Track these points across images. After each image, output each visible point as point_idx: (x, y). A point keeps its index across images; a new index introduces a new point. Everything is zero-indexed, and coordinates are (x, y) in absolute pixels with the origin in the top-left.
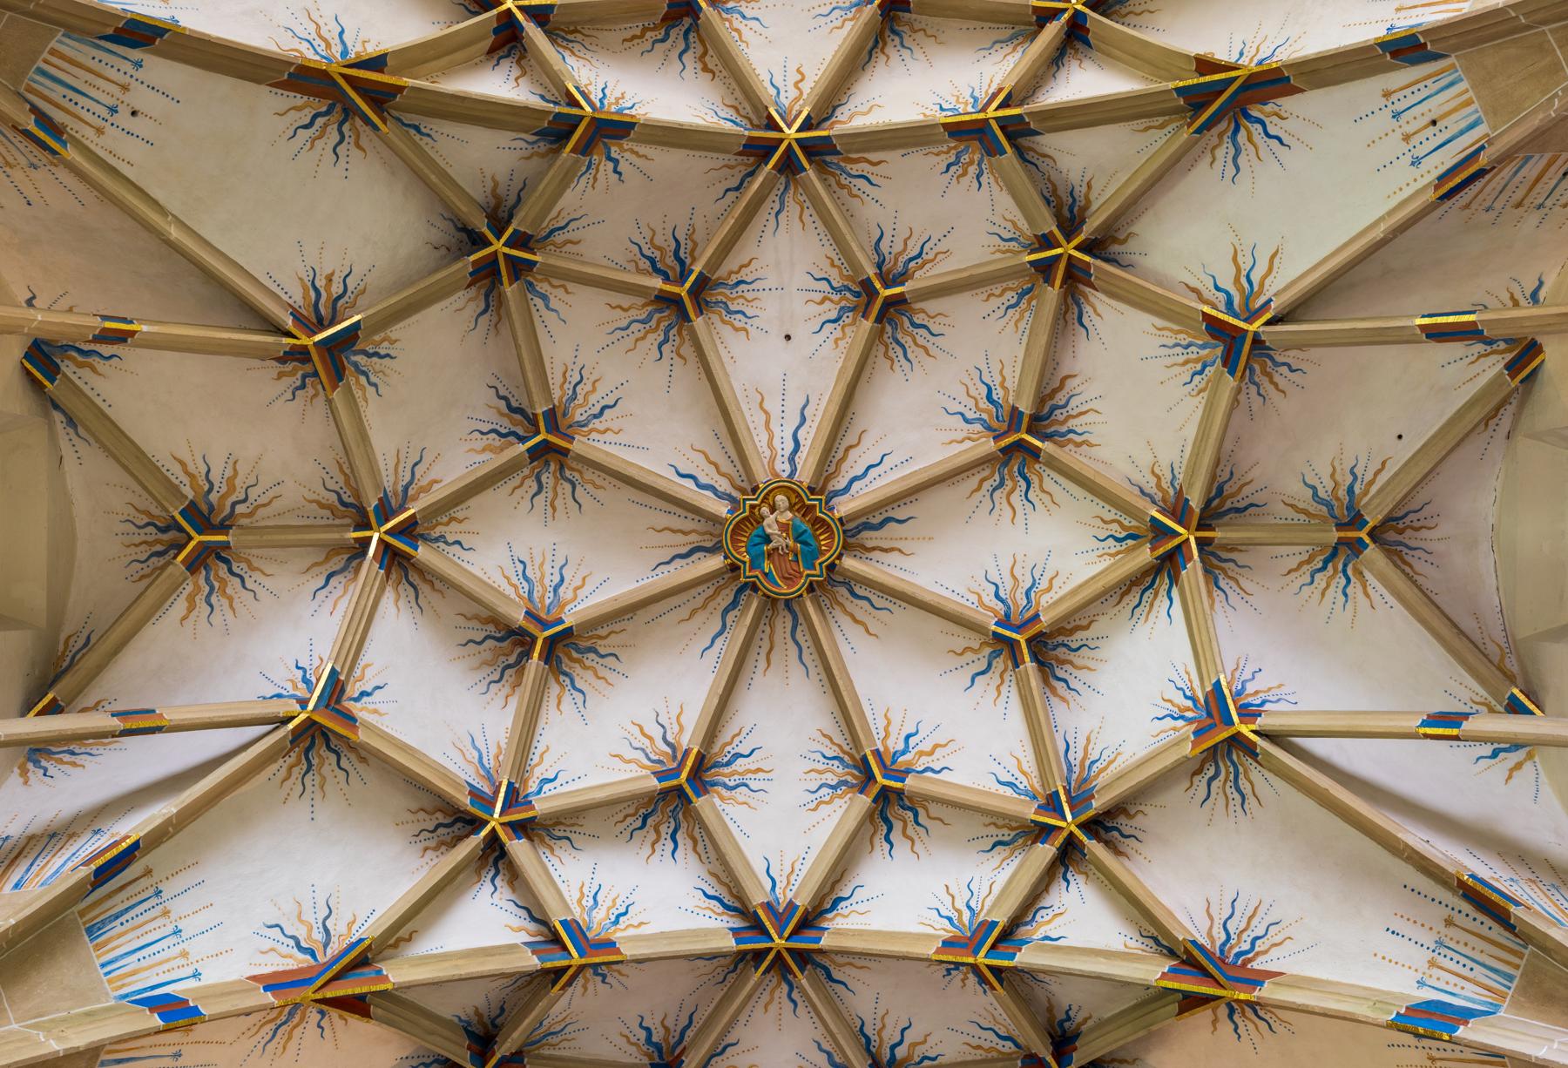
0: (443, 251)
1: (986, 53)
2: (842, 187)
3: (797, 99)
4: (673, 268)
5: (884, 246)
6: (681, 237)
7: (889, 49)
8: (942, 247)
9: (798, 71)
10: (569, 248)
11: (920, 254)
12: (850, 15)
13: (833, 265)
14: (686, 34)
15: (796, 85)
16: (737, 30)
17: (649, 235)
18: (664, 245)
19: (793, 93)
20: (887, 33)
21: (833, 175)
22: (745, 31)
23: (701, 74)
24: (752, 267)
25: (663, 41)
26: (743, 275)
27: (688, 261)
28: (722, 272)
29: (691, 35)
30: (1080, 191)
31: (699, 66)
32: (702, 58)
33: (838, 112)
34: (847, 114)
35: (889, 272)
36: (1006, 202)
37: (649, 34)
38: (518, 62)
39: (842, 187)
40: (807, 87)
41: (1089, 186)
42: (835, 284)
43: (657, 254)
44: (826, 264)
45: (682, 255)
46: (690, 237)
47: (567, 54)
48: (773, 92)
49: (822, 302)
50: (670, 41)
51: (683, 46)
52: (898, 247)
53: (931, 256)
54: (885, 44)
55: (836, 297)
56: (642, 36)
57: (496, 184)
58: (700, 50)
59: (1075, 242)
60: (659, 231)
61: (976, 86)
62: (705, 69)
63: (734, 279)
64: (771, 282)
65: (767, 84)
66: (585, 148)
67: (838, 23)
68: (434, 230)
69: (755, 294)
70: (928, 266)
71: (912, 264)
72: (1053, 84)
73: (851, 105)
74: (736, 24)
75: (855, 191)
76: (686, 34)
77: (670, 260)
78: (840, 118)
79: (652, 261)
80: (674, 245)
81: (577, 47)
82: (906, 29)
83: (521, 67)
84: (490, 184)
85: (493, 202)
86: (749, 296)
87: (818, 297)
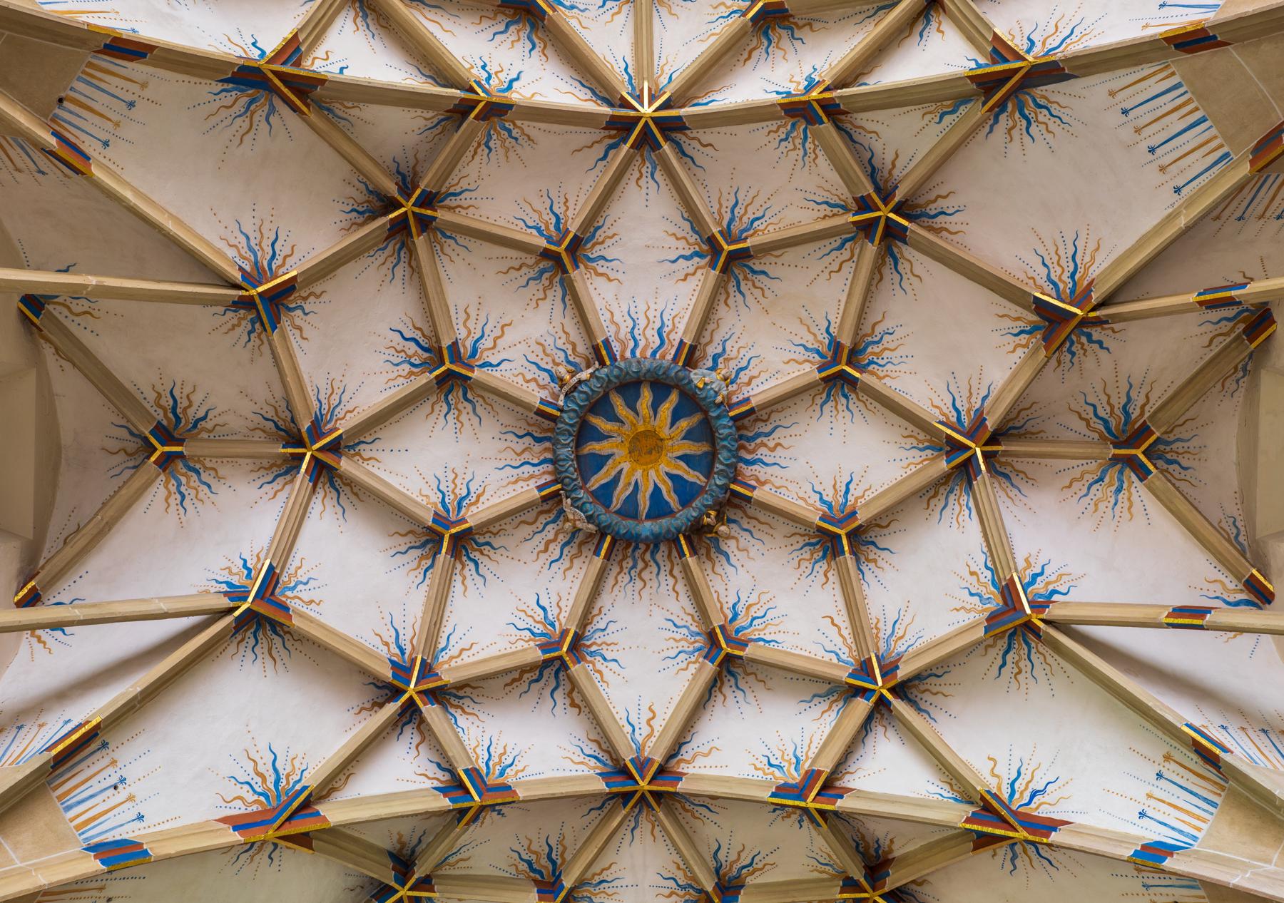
0: (358, 890)
1: (806, 705)
2: (687, 811)
3: (649, 736)
4: (546, 867)
5: (721, 855)
6: (553, 842)
7: (726, 690)
8: (769, 860)
9: (650, 709)
10: (461, 864)
11: (751, 864)
12: (693, 659)
13: (679, 868)
14: (557, 673)
15: (649, 721)
16: (599, 672)
17: (526, 843)
18: (539, 850)
19: (646, 730)
20: (725, 673)
21: (679, 802)
22: (605, 672)
23: (570, 709)
24: (612, 870)
25: (537, 681)
26: (604, 876)
27: (559, 862)
28: (589, 875)
29: (561, 674)
30: (885, 843)
31: (568, 701)
32: (570, 694)
33: (683, 751)
34: (691, 753)
35: (725, 875)
36: (820, 842)
37: (526, 676)
38: (418, 728)
39: (687, 811)
40: (658, 725)
41: (892, 841)
42: (680, 883)
43: (534, 857)
44: (673, 868)
45: (554, 857)
46: (560, 842)
47: (458, 713)
48: (628, 729)
49: (669, 896)
50: (543, 681)
51: (554, 685)
52: (733, 857)
53: (760, 866)
54: (722, 683)
55: (681, 893)
56: (520, 679)
57: (401, 836)
58: (568, 687)
59: (879, 892)
60: (535, 840)
61: (798, 740)
62: (573, 705)
63: (597, 879)
64: (628, 880)
65: (623, 722)
66: (475, 818)
67: (683, 665)
68: (350, 878)
69: (614, 890)
70: (757, 873)
71: (744, 871)
72: (861, 751)
73: (693, 744)
74: (598, 666)
75: (697, 815)
76: (557, 673)
77: (544, 861)
78: (686, 757)
79: (529, 863)
80: (547, 849)
81: (467, 702)
82: (740, 670)
83: (421, 733)
84: (395, 838)
85: (398, 846)
86: (610, 891)
87: (667, 892)
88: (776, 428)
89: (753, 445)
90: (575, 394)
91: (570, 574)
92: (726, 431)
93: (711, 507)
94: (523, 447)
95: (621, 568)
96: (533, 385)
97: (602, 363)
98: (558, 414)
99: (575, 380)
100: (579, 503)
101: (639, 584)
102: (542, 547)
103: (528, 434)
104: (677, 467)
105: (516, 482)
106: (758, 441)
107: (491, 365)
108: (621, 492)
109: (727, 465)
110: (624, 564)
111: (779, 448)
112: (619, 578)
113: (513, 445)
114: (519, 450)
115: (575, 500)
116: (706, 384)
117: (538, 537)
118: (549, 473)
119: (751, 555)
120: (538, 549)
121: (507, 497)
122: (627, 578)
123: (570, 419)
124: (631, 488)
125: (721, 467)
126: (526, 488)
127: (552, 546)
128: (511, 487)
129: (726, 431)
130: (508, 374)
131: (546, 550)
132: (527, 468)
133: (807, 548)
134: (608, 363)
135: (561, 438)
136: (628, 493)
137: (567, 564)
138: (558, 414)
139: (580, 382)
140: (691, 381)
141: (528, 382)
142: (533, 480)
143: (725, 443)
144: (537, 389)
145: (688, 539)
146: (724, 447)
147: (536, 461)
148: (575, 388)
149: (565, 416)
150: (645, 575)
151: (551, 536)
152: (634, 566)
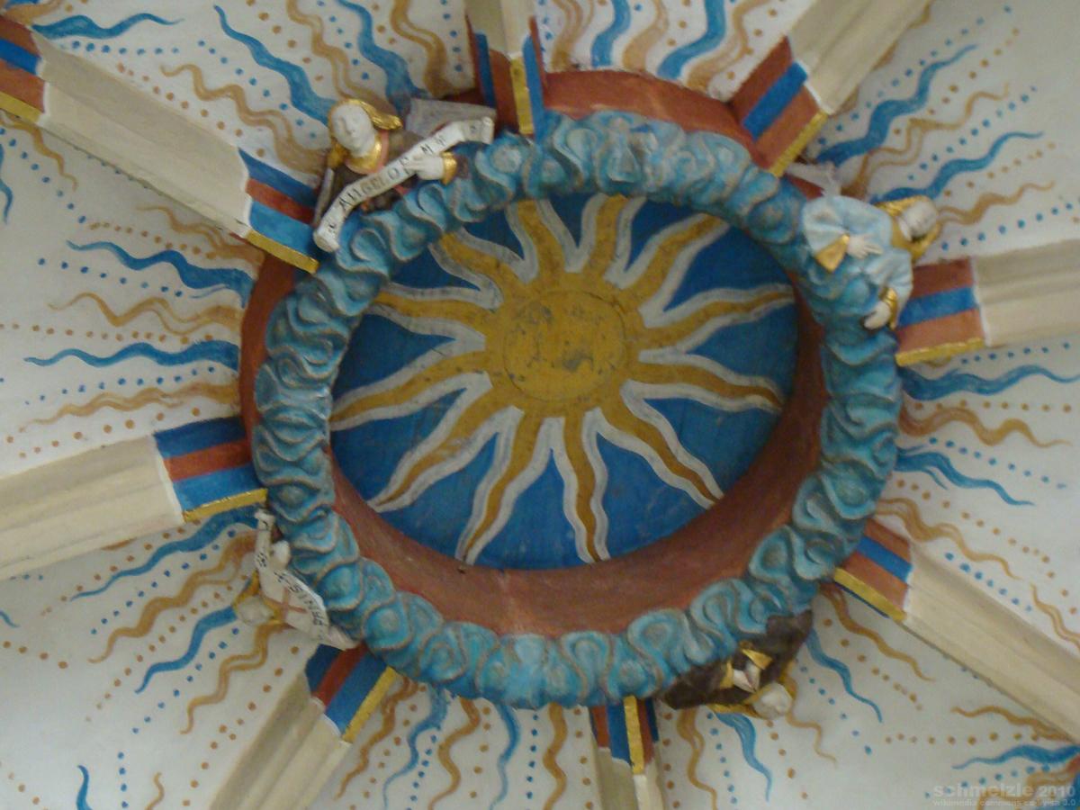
88: (1024, 372)
89: (929, 407)
90: (389, 220)
91: (211, 717)
92: (874, 418)
93: (756, 642)
94: (140, 295)
95: (389, 722)
96: (224, 110)
97: (506, 125)
98: (310, 266)
99: (396, 173)
100: (318, 569)
101: (436, 778)
102: (132, 618)
103: (169, 256)
104: (646, 432)
105: (90, 409)
106: (953, 399)
107: (90, 29)
108: (430, 461)
109: (847, 525)
110: (402, 710)
111: (1016, 438)
112: (375, 755)
113: (106, 289)
114: (121, 305)
115: (300, 559)
116: (848, 258)
117: (128, 586)
118: (212, 391)
119: (829, 744)
120: (116, 624)
121: (49, 457)
122: (403, 753)
123: (352, 297)
124: (466, 457)
125: (824, 524)
126: (120, 435)
127: (164, 620)
128: (69, 425)
129: (874, 418)
130: (141, 66)
131: (145, 627)
132: (143, 368)
133: (1021, 763)
134: (527, 127)
135: (306, 357)
136: (450, 467)
137: (205, 683)
138: (310, 266)
139: (414, 182)
140: (800, 239)
141: (208, 95)
142: (152, 409)
143: (862, 455)
144: (234, 122)
145: (647, 710)
146: (854, 464)
147: (173, 346)
148: (392, 199)
149: (329, 279)
150: (464, 754)
151: (171, 587)
152: (433, 722)
